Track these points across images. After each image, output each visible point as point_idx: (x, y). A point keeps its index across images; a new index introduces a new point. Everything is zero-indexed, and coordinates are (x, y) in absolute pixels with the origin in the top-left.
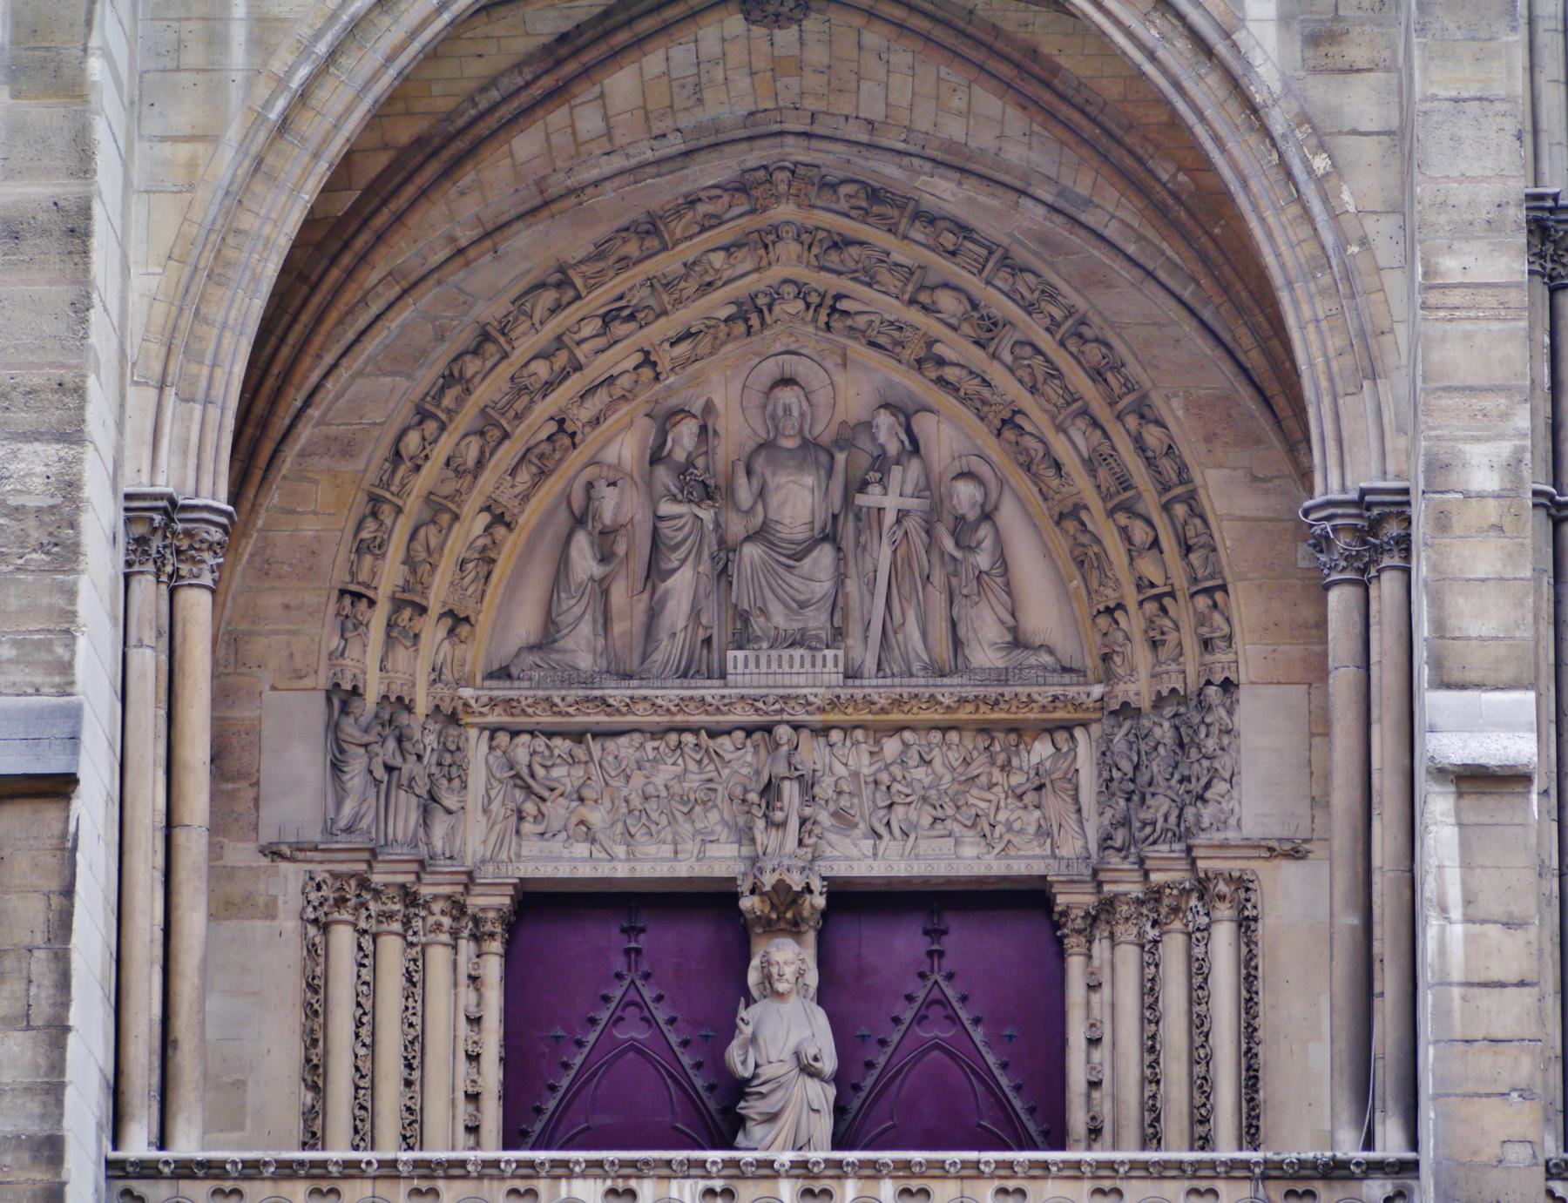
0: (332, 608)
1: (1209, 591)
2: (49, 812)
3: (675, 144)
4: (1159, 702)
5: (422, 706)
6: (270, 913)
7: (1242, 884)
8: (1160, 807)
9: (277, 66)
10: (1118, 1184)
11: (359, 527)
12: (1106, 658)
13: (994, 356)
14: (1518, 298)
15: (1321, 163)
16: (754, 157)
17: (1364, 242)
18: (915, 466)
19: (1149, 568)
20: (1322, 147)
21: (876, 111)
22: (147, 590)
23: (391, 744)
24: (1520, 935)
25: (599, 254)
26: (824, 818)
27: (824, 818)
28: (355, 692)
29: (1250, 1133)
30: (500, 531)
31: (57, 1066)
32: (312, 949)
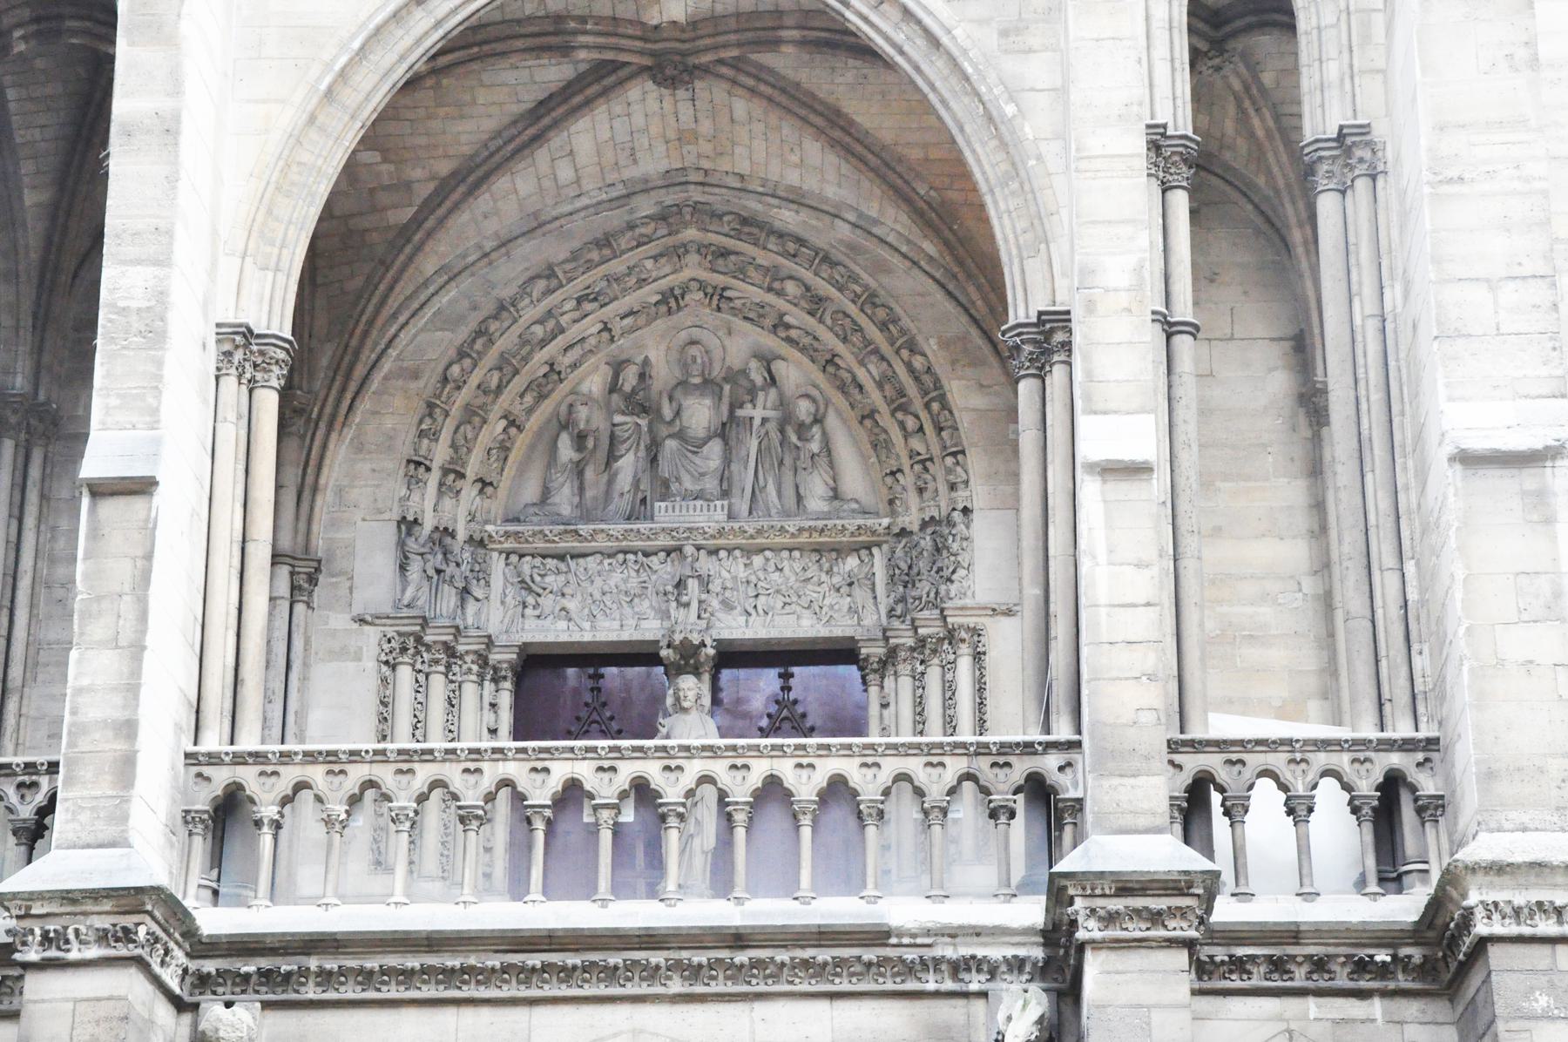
0: (402, 472)
1: (954, 454)
2: (138, 503)
3: (620, 190)
4: (924, 525)
5: (462, 535)
6: (358, 657)
7: (976, 632)
8: (923, 588)
10: (878, 759)
11: (421, 422)
12: (891, 502)
13: (821, 321)
16: (670, 198)
17: (1039, 158)
18: (773, 392)
19: (916, 444)
20: (1012, 99)
21: (744, 167)
22: (229, 383)
23: (440, 556)
24: (1147, 573)
25: (575, 256)
26: (715, 603)
27: (715, 603)
30: (513, 431)
31: (136, 672)
32: (384, 680)
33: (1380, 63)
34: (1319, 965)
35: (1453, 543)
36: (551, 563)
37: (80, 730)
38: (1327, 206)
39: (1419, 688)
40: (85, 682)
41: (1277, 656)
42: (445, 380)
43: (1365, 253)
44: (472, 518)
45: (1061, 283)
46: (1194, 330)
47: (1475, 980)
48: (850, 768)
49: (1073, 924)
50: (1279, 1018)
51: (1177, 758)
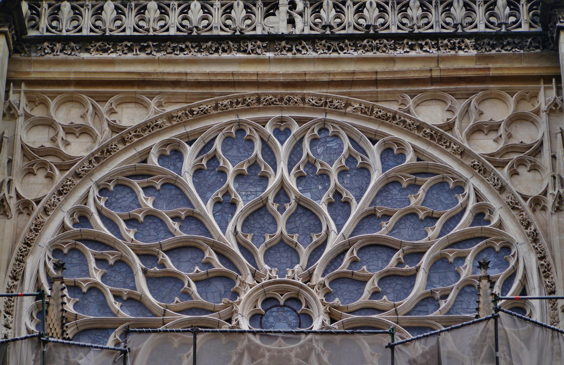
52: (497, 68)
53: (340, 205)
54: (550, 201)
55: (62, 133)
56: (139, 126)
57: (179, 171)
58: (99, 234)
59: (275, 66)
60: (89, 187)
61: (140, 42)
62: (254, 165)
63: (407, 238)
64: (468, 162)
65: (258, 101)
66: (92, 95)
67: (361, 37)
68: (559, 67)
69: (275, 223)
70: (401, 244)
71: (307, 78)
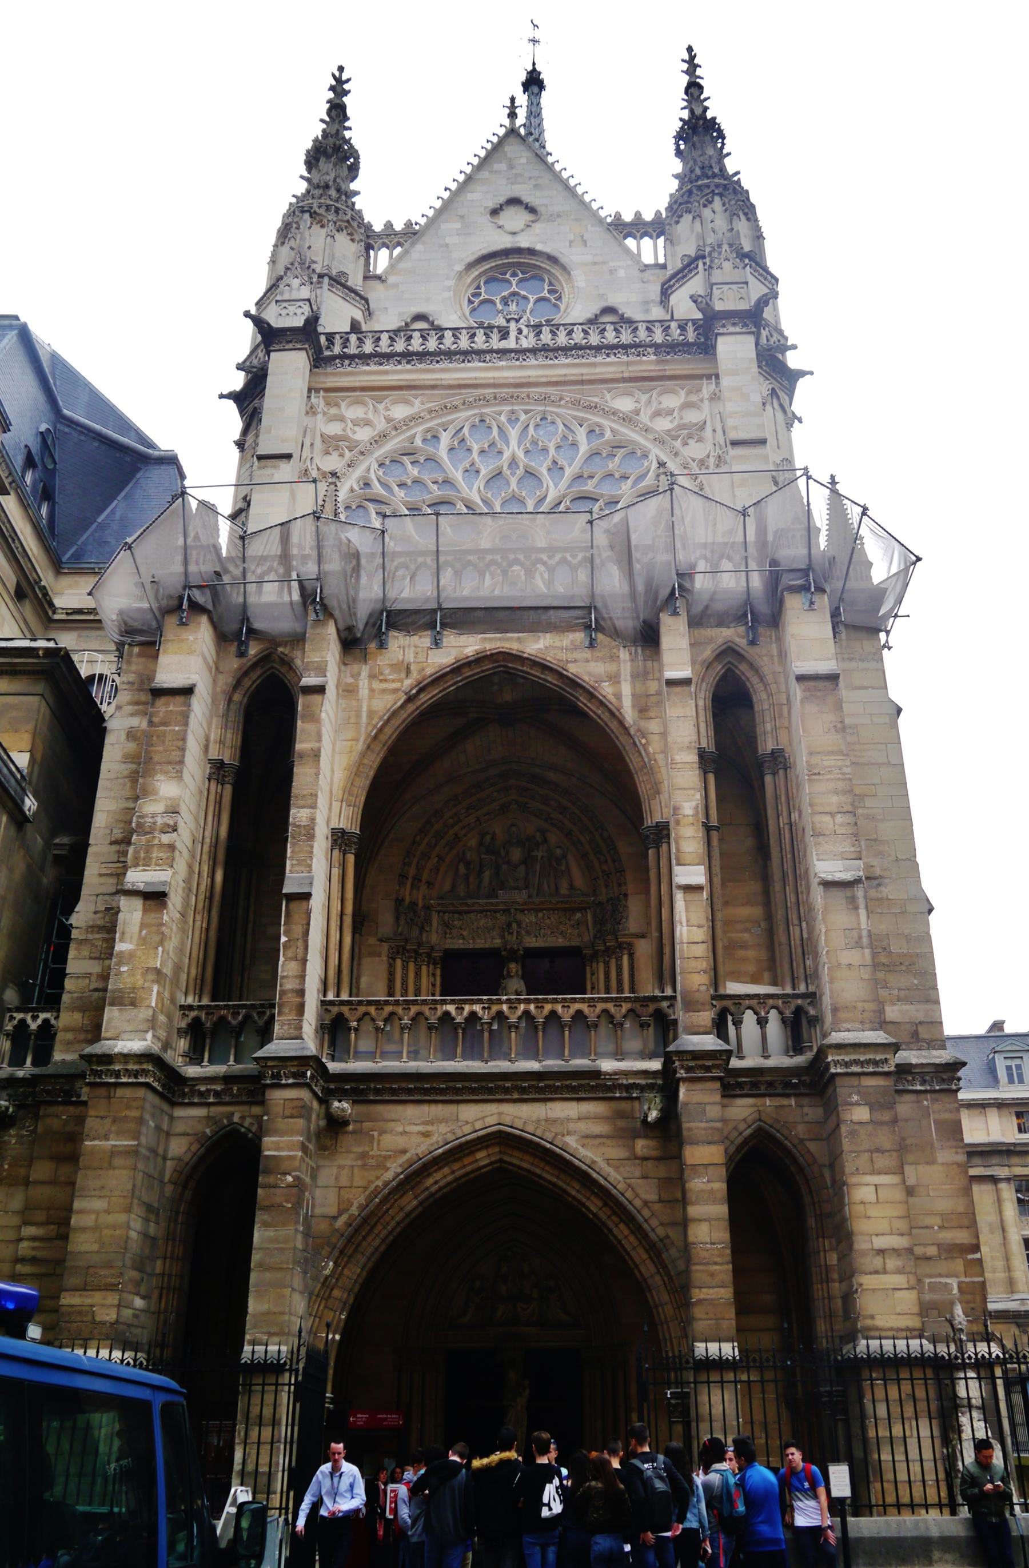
2: (304, 904)
4: (608, 900)
6: (380, 956)
8: (608, 926)
9: (374, 722)
14: (697, 765)
15: (644, 741)
17: (655, 760)
20: (644, 737)
22: (336, 852)
26: (523, 933)
27: (523, 933)
28: (403, 900)
29: (632, 990)
31: (304, 970)
32: (390, 965)
33: (787, 725)
34: (770, 1084)
35: (820, 917)
36: (456, 916)
37: (283, 993)
38: (768, 779)
39: (808, 973)
40: (285, 974)
41: (751, 953)
42: (414, 842)
43: (783, 799)
44: (424, 898)
45: (665, 810)
46: (717, 829)
47: (830, 1091)
48: (584, 1007)
49: (675, 1072)
50: (755, 1105)
51: (714, 1002)
52: (671, 369)
53: (556, 468)
54: (712, 461)
55: (350, 425)
56: (407, 417)
57: (438, 450)
58: (378, 495)
59: (506, 372)
60: (370, 462)
61: (407, 356)
62: (493, 444)
63: (607, 490)
64: (651, 437)
65: (495, 398)
66: (373, 398)
67: (571, 349)
68: (717, 368)
69: (508, 483)
70: (602, 495)
71: (531, 380)
